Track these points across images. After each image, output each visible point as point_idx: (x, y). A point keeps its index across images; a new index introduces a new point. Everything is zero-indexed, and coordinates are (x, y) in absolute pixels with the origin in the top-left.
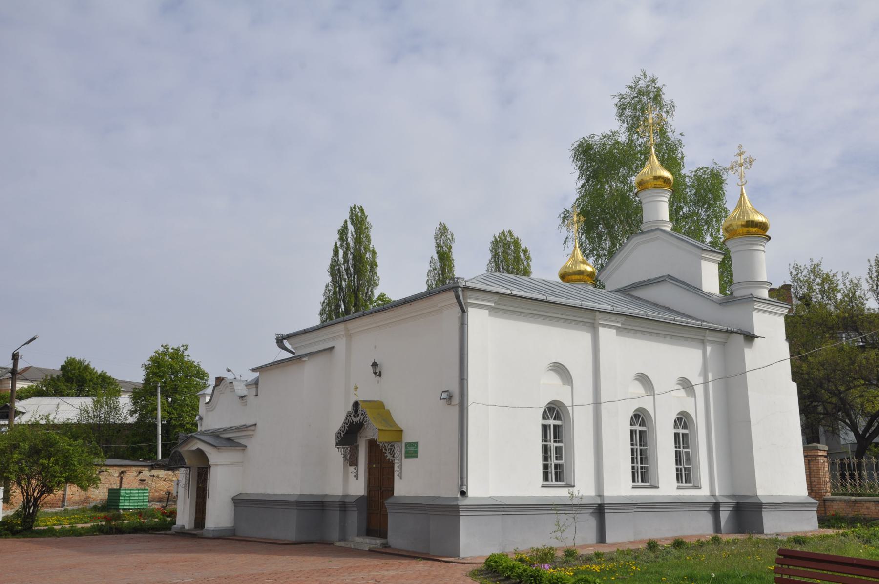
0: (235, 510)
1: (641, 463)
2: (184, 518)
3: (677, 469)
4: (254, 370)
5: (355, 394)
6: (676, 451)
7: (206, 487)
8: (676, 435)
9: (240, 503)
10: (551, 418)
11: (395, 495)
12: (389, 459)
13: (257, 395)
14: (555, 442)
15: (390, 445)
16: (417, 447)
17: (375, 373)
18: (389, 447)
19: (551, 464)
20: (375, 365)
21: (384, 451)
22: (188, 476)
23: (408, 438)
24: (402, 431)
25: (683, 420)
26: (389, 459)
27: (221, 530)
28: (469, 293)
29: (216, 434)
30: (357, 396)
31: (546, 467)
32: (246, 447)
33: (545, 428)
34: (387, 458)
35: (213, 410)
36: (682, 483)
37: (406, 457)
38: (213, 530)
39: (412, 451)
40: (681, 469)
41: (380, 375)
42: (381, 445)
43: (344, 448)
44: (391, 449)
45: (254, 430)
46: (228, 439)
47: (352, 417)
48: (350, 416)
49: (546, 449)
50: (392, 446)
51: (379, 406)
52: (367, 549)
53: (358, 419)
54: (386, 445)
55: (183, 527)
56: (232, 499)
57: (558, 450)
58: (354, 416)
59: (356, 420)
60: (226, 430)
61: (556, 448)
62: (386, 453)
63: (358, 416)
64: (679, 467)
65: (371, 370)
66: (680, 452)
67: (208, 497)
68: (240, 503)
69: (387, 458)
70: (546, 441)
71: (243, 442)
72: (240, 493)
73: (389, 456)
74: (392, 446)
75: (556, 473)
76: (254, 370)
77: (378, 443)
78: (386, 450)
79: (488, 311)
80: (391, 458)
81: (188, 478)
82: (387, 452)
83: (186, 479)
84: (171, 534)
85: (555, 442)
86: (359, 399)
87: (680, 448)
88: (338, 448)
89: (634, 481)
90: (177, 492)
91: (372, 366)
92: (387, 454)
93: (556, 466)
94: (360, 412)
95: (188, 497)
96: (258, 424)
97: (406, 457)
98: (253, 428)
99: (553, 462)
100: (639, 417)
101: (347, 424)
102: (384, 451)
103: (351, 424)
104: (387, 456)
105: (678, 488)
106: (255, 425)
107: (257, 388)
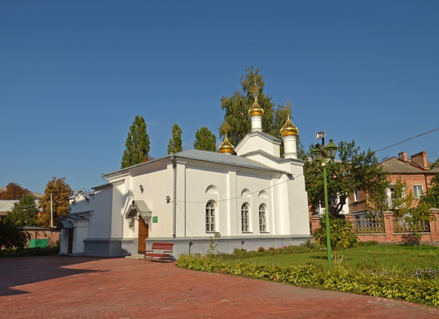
0: (85, 245)
1: (246, 223)
2: (64, 250)
3: (260, 226)
4: (92, 189)
5: (134, 199)
6: (260, 219)
7: (73, 236)
8: (260, 212)
9: (86, 242)
11: (149, 237)
12: (146, 223)
13: (93, 199)
15: (147, 218)
16: (157, 218)
18: (146, 218)
20: (141, 186)
21: (144, 220)
22: (65, 232)
23: (153, 215)
25: (262, 206)
26: (146, 223)
27: (79, 253)
28: (177, 158)
29: (76, 215)
30: (134, 199)
31: (208, 225)
32: (89, 220)
33: (207, 210)
35: (75, 205)
36: (262, 231)
37: (153, 223)
38: (76, 254)
39: (156, 220)
40: (262, 225)
42: (143, 218)
43: (129, 219)
44: (147, 219)
45: (92, 213)
46: (82, 217)
47: (132, 207)
48: (131, 206)
49: (207, 218)
50: (147, 218)
51: (143, 202)
52: (137, 258)
53: (134, 208)
54: (145, 218)
55: (63, 253)
56: (84, 241)
58: (133, 207)
59: (133, 208)
60: (81, 213)
61: (212, 218)
62: (145, 221)
63: (134, 206)
64: (261, 225)
65: (140, 188)
66: (261, 219)
67: (74, 240)
68: (86, 242)
70: (208, 215)
71: (88, 218)
72: (87, 239)
73: (146, 222)
74: (147, 218)
75: (212, 228)
76: (92, 189)
77: (142, 217)
78: (145, 219)
79: (185, 165)
80: (147, 223)
81: (65, 233)
82: (146, 220)
83: (64, 233)
84: (59, 256)
85: (211, 215)
86: (134, 200)
87: (261, 217)
88: (127, 220)
89: (243, 230)
91: (140, 186)
92: (146, 221)
93: (212, 225)
94: (135, 205)
95: (65, 241)
96: (94, 211)
97: (153, 223)
98: (92, 212)
99: (210, 223)
100: (244, 205)
101: (130, 210)
102: (144, 220)
103: (132, 210)
104: (145, 222)
105: (261, 233)
106: (93, 211)
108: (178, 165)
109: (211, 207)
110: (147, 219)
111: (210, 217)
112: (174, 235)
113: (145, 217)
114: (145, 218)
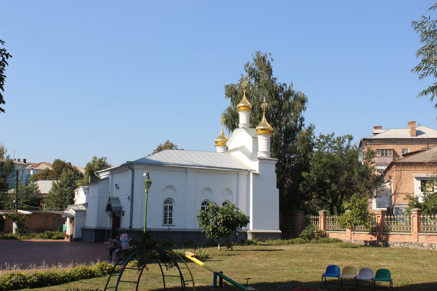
10: (168, 203)
13: (88, 193)
14: (169, 211)
17: (117, 188)
19: (167, 219)
20: (116, 185)
24: (122, 207)
34: (116, 216)
41: (118, 188)
42: (114, 212)
44: (118, 213)
54: (116, 212)
57: (171, 214)
61: (170, 213)
69: (116, 216)
70: (166, 211)
78: (116, 213)
90: (66, 226)
93: (169, 219)
96: (88, 203)
99: (168, 217)
107: (88, 190)
108: (136, 171)
109: (170, 204)
110: (118, 213)
111: (168, 212)
112: (130, 227)
113: (116, 211)
114: (116, 212)
